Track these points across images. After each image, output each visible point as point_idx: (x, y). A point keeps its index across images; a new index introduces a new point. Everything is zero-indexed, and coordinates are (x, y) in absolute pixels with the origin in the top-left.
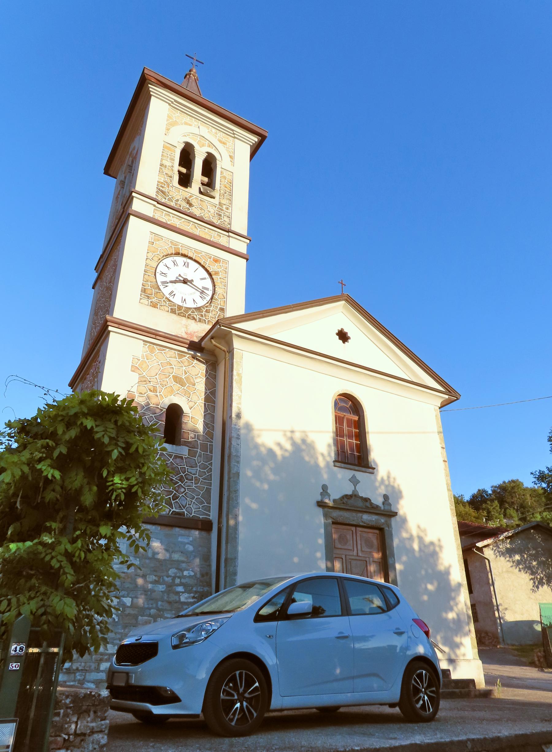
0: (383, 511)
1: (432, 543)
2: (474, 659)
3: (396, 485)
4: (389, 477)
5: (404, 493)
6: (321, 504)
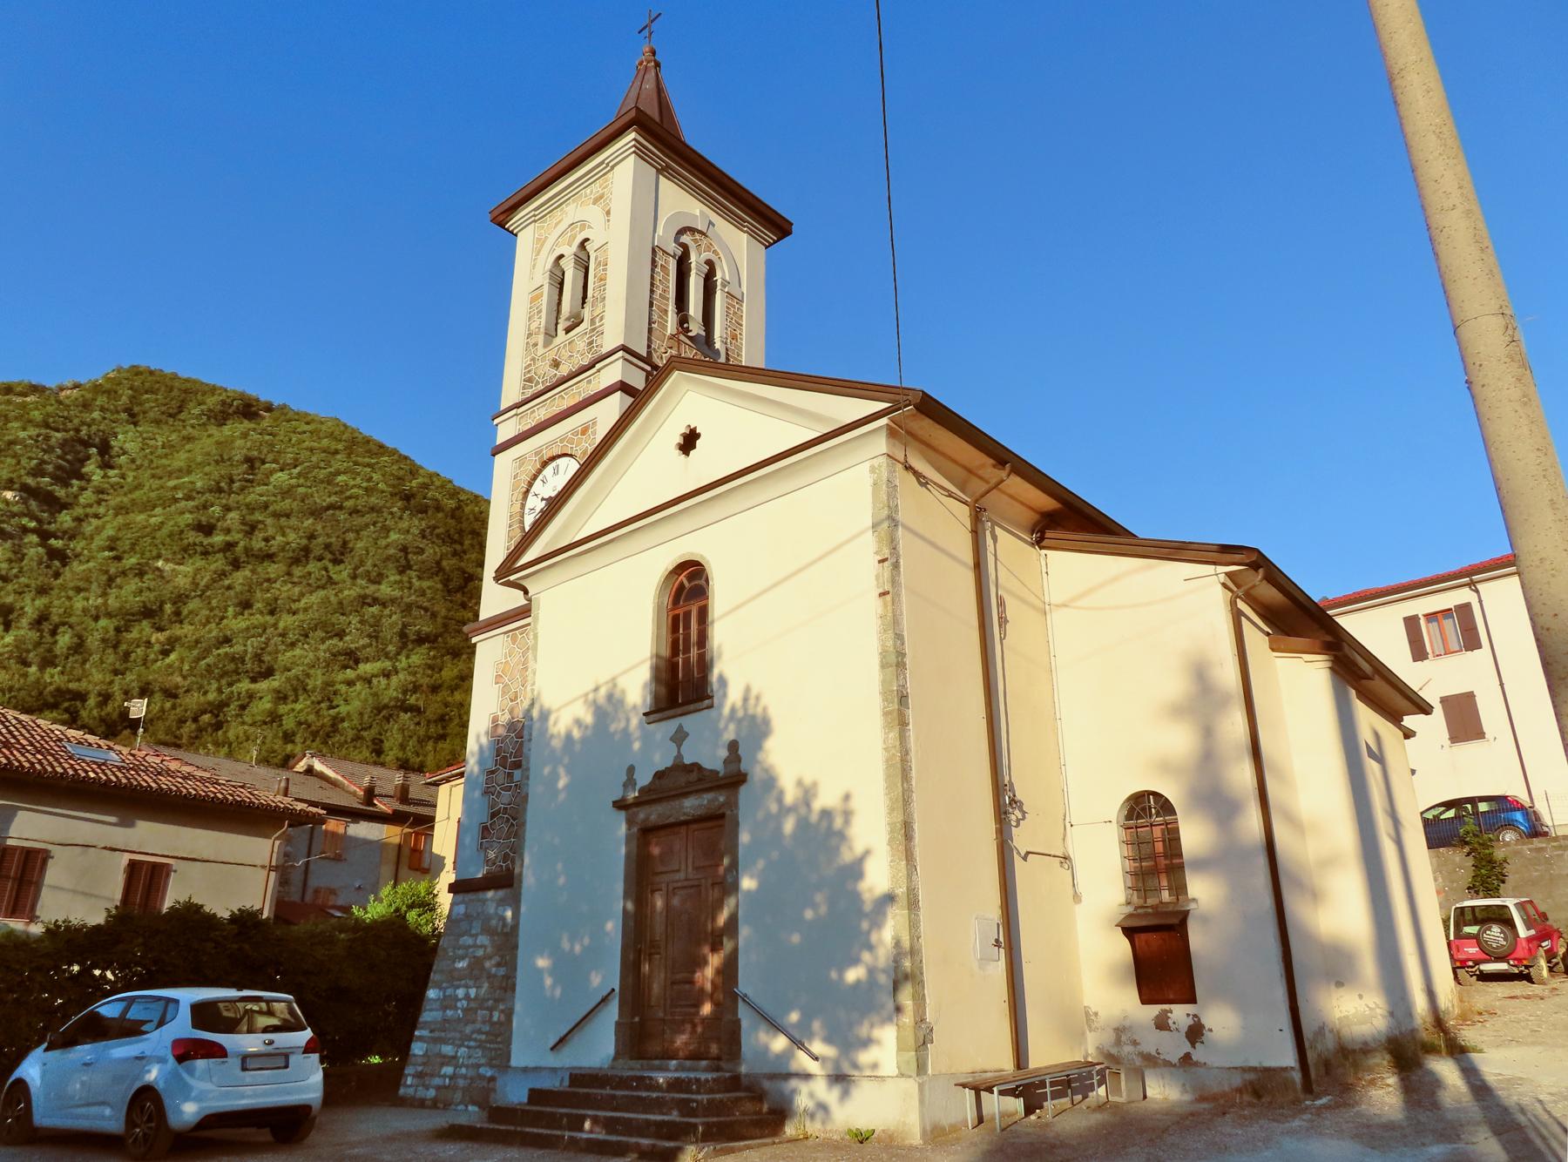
0: (724, 778)
1: (826, 814)
2: (902, 1075)
3: (759, 710)
4: (746, 700)
5: (776, 723)
6: (620, 805)
